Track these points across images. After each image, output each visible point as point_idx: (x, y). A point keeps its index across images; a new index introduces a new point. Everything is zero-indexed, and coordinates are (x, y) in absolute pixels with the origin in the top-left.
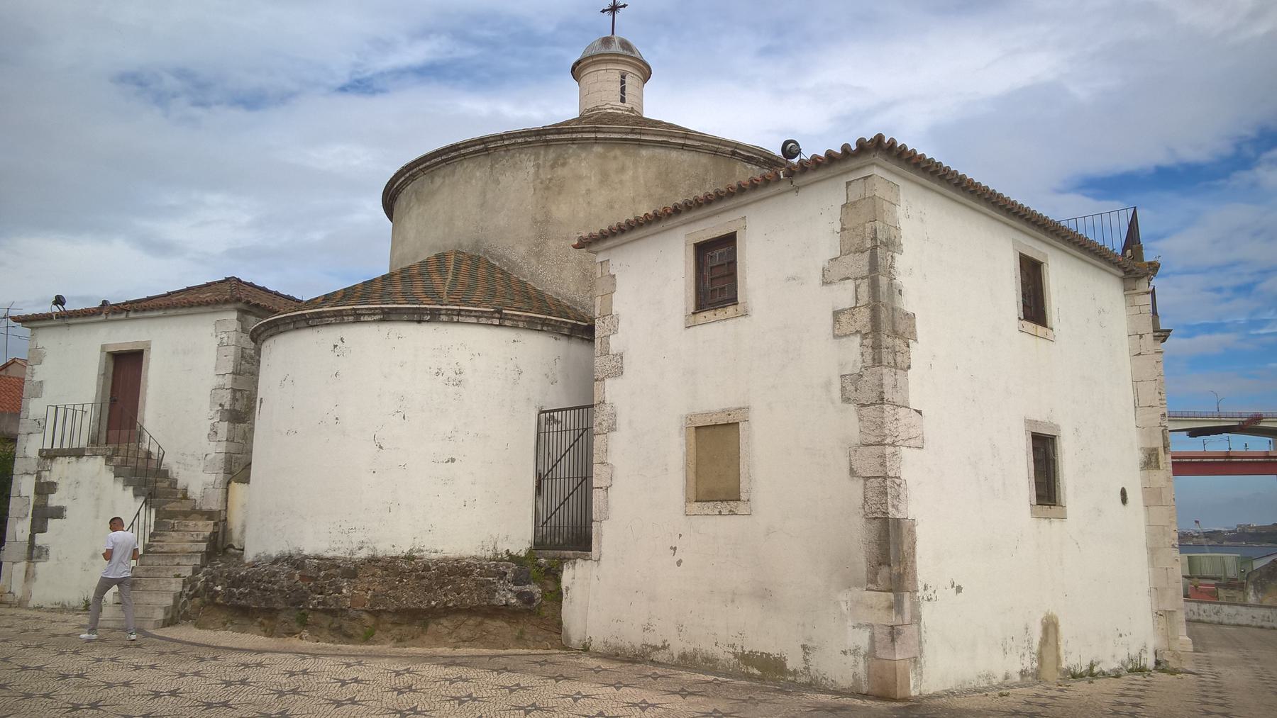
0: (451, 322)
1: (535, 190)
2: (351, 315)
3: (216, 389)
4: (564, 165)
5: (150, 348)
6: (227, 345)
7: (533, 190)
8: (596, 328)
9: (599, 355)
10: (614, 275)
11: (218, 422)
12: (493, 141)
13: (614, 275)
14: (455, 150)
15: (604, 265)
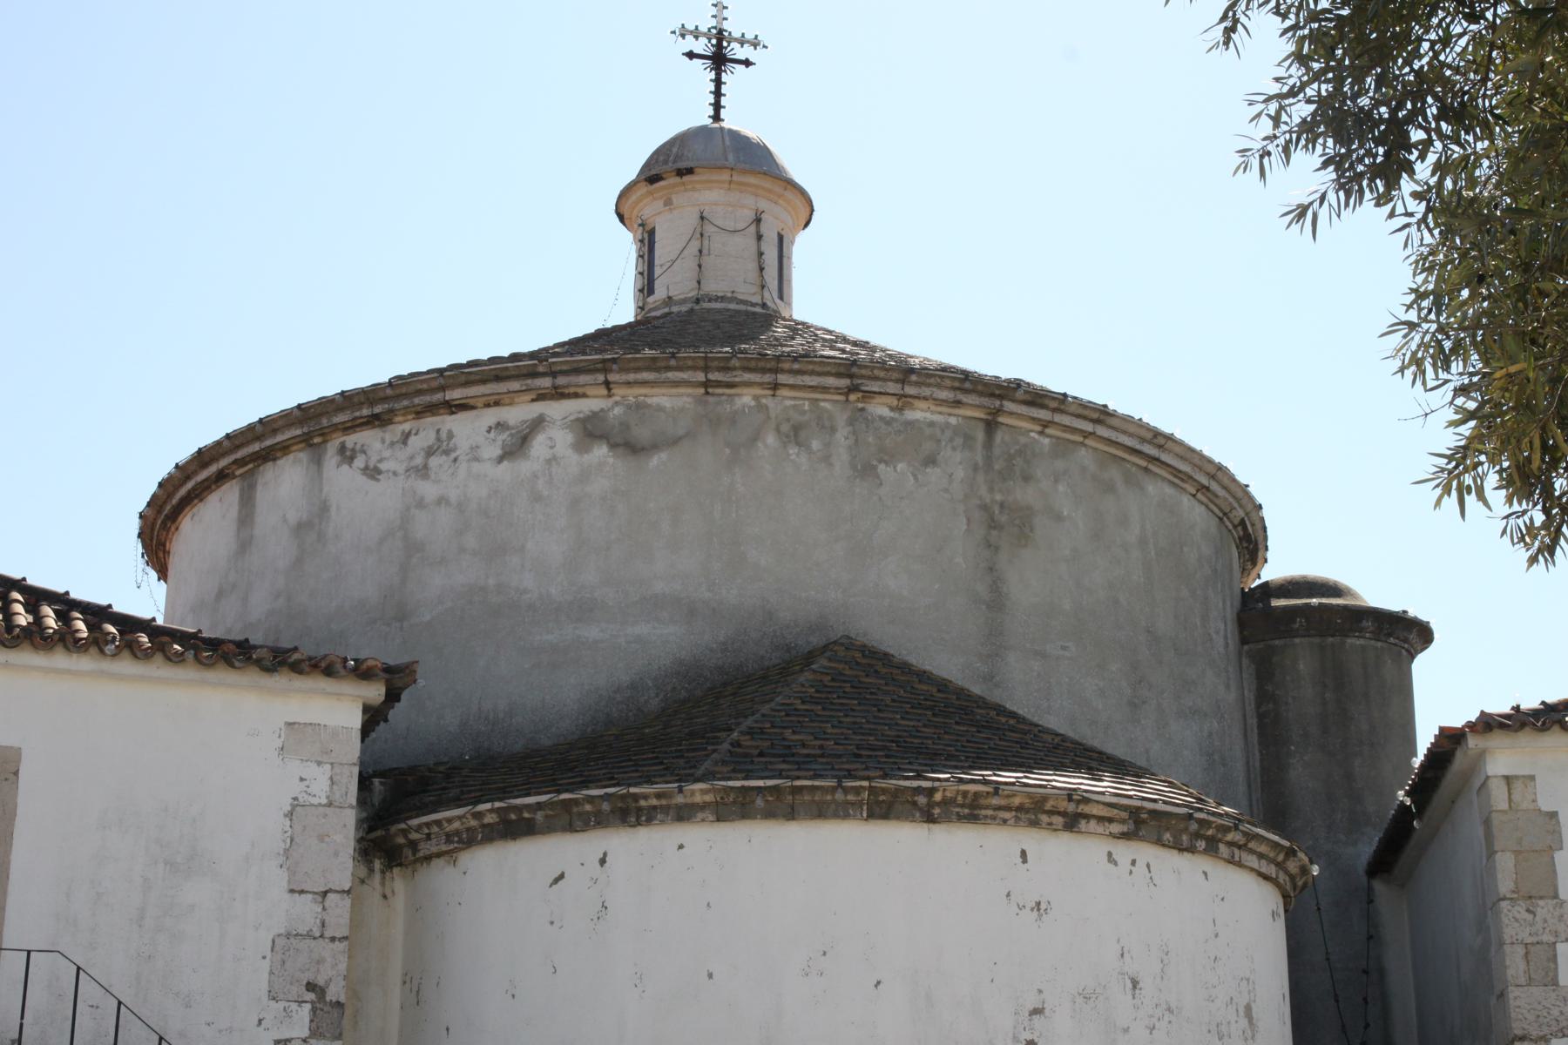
0: (1231, 861)
1: (968, 520)
2: (1059, 813)
3: (288, 936)
4: (1027, 478)
5: (16, 773)
6: (330, 804)
7: (965, 520)
8: (1505, 920)
9: (1522, 980)
10: (1553, 815)
11: (304, 1041)
12: (876, 378)
13: (1553, 815)
14: (764, 371)
15: (1518, 786)
